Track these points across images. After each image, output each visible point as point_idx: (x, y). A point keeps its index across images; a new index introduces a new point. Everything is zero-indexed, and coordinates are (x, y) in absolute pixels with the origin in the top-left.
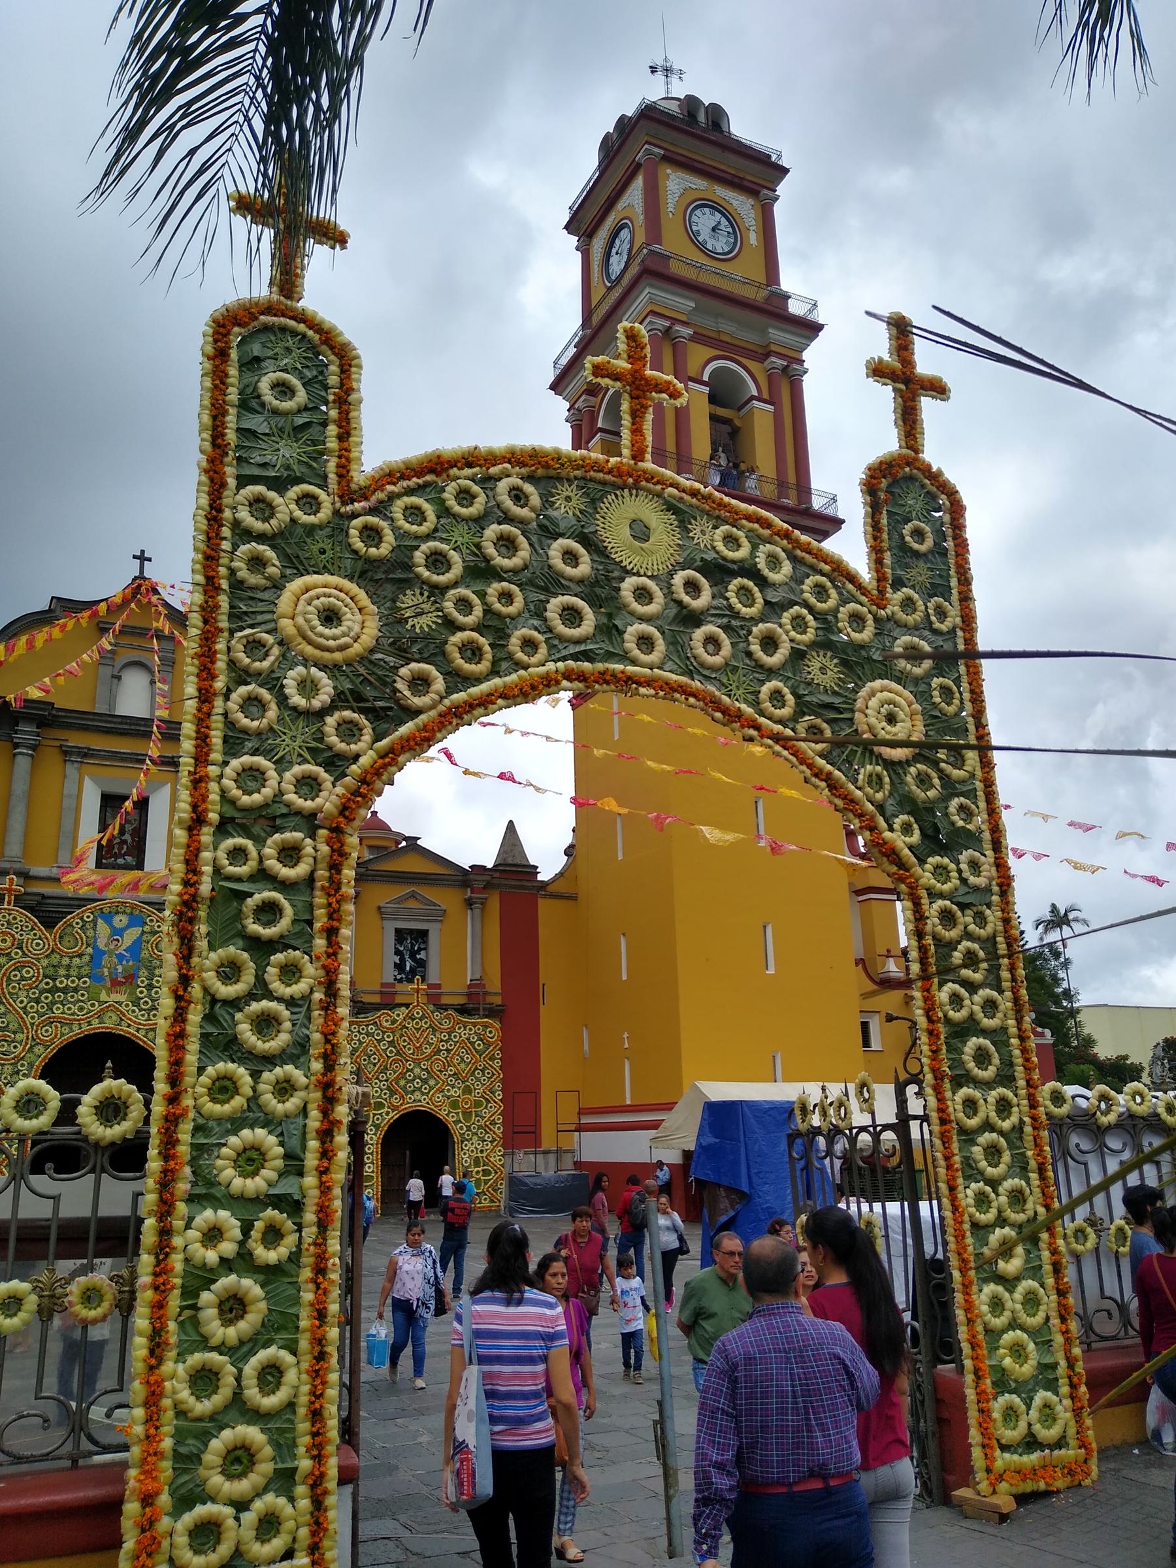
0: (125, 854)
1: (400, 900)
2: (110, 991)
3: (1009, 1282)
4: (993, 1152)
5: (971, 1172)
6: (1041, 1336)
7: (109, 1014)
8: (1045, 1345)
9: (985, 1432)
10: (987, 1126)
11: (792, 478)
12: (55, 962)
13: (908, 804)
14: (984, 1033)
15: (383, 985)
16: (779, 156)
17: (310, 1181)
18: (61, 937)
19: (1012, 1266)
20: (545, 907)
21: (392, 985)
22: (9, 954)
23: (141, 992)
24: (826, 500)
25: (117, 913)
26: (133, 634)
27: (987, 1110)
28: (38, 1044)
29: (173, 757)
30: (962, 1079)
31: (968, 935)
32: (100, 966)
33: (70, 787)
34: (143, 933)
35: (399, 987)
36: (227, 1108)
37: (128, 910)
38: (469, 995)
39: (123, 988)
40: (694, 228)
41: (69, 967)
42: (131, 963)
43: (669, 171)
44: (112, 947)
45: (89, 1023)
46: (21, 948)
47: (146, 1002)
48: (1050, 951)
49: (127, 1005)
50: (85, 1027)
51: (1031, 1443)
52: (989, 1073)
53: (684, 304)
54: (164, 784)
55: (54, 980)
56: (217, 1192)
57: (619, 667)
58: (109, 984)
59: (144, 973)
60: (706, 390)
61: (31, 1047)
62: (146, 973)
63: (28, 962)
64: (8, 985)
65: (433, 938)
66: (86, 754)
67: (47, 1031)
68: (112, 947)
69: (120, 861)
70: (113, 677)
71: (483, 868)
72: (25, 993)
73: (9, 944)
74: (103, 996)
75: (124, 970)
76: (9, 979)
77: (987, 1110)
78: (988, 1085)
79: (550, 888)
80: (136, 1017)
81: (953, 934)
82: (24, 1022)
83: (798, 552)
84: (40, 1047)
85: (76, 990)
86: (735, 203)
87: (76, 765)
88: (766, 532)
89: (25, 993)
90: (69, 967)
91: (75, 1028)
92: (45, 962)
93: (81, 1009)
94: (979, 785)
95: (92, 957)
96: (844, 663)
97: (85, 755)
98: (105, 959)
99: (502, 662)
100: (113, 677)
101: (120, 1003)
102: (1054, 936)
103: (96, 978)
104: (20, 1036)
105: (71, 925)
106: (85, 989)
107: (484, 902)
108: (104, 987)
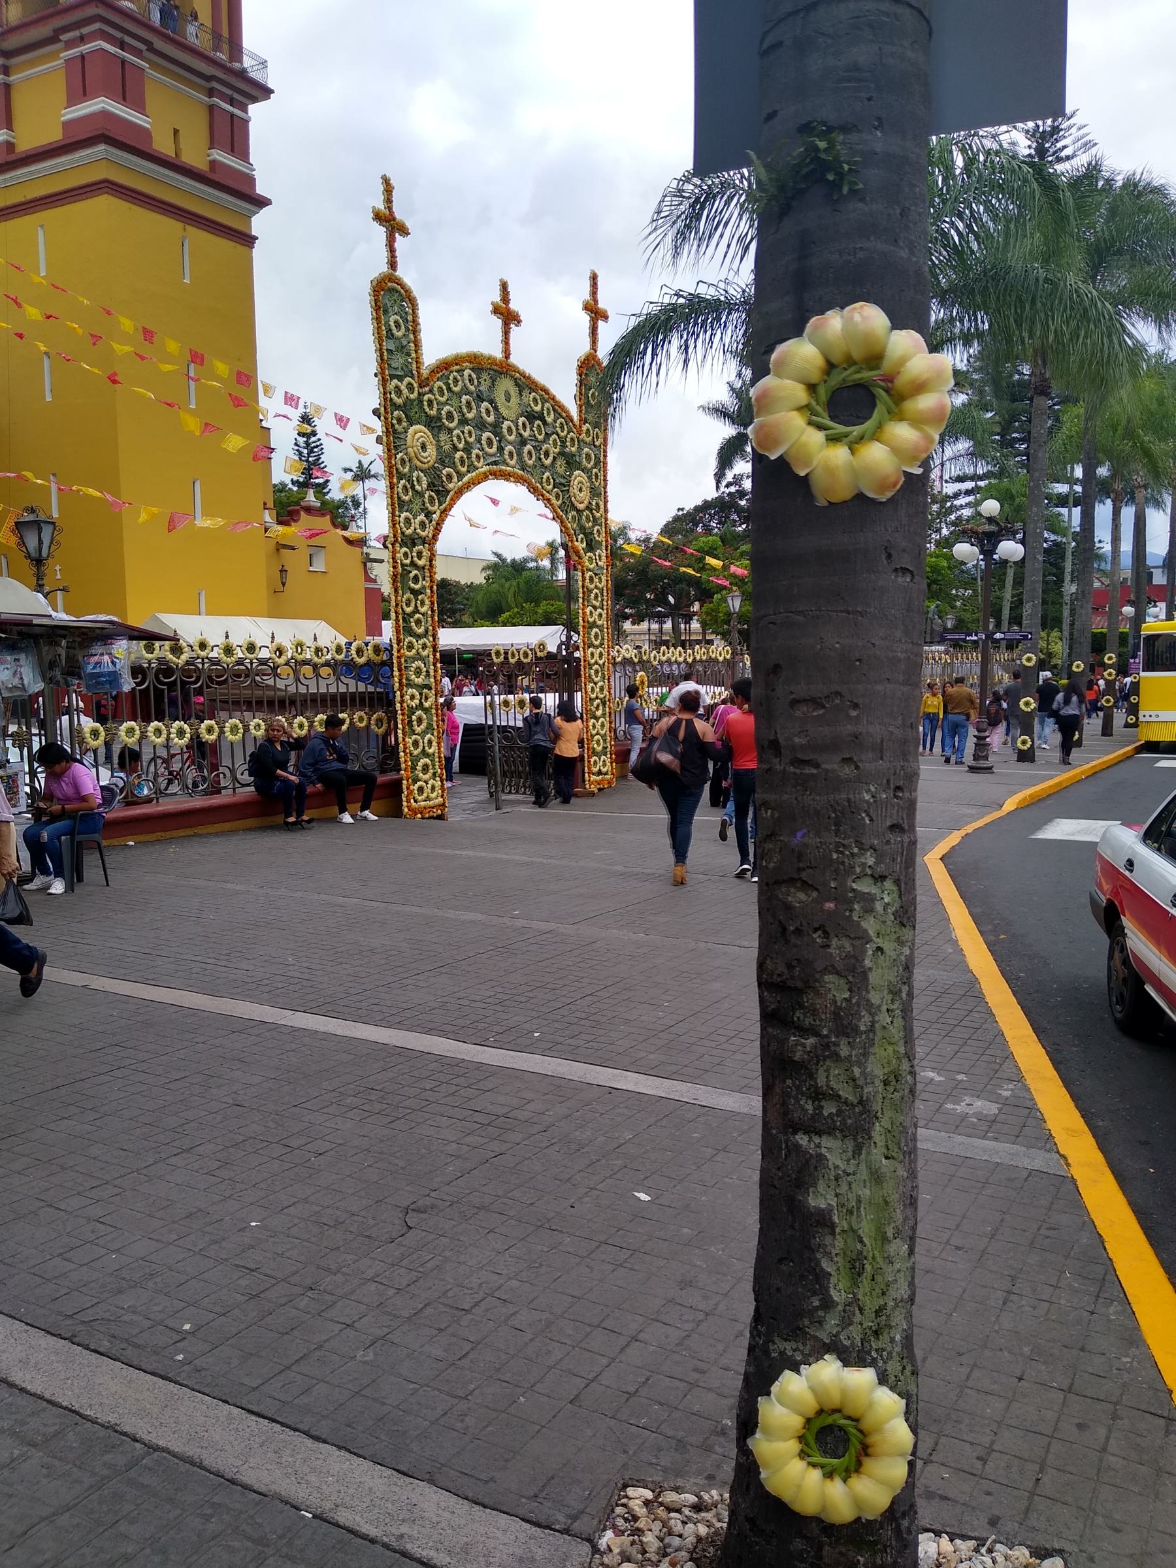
3: (597, 719)
4: (597, 672)
5: (591, 681)
6: (604, 737)
8: (605, 741)
9: (589, 769)
10: (596, 663)
11: (225, 33)
13: (583, 529)
14: (597, 627)
17: (432, 680)
19: (599, 713)
24: (256, 63)
27: (596, 656)
30: (591, 645)
31: (596, 587)
36: (411, 653)
48: (353, 501)
51: (600, 773)
52: (597, 643)
56: (412, 683)
57: (503, 468)
77: (596, 656)
78: (596, 647)
81: (592, 586)
83: (556, 407)
88: (547, 396)
94: (603, 520)
96: (567, 463)
99: (472, 468)
102: (358, 490)
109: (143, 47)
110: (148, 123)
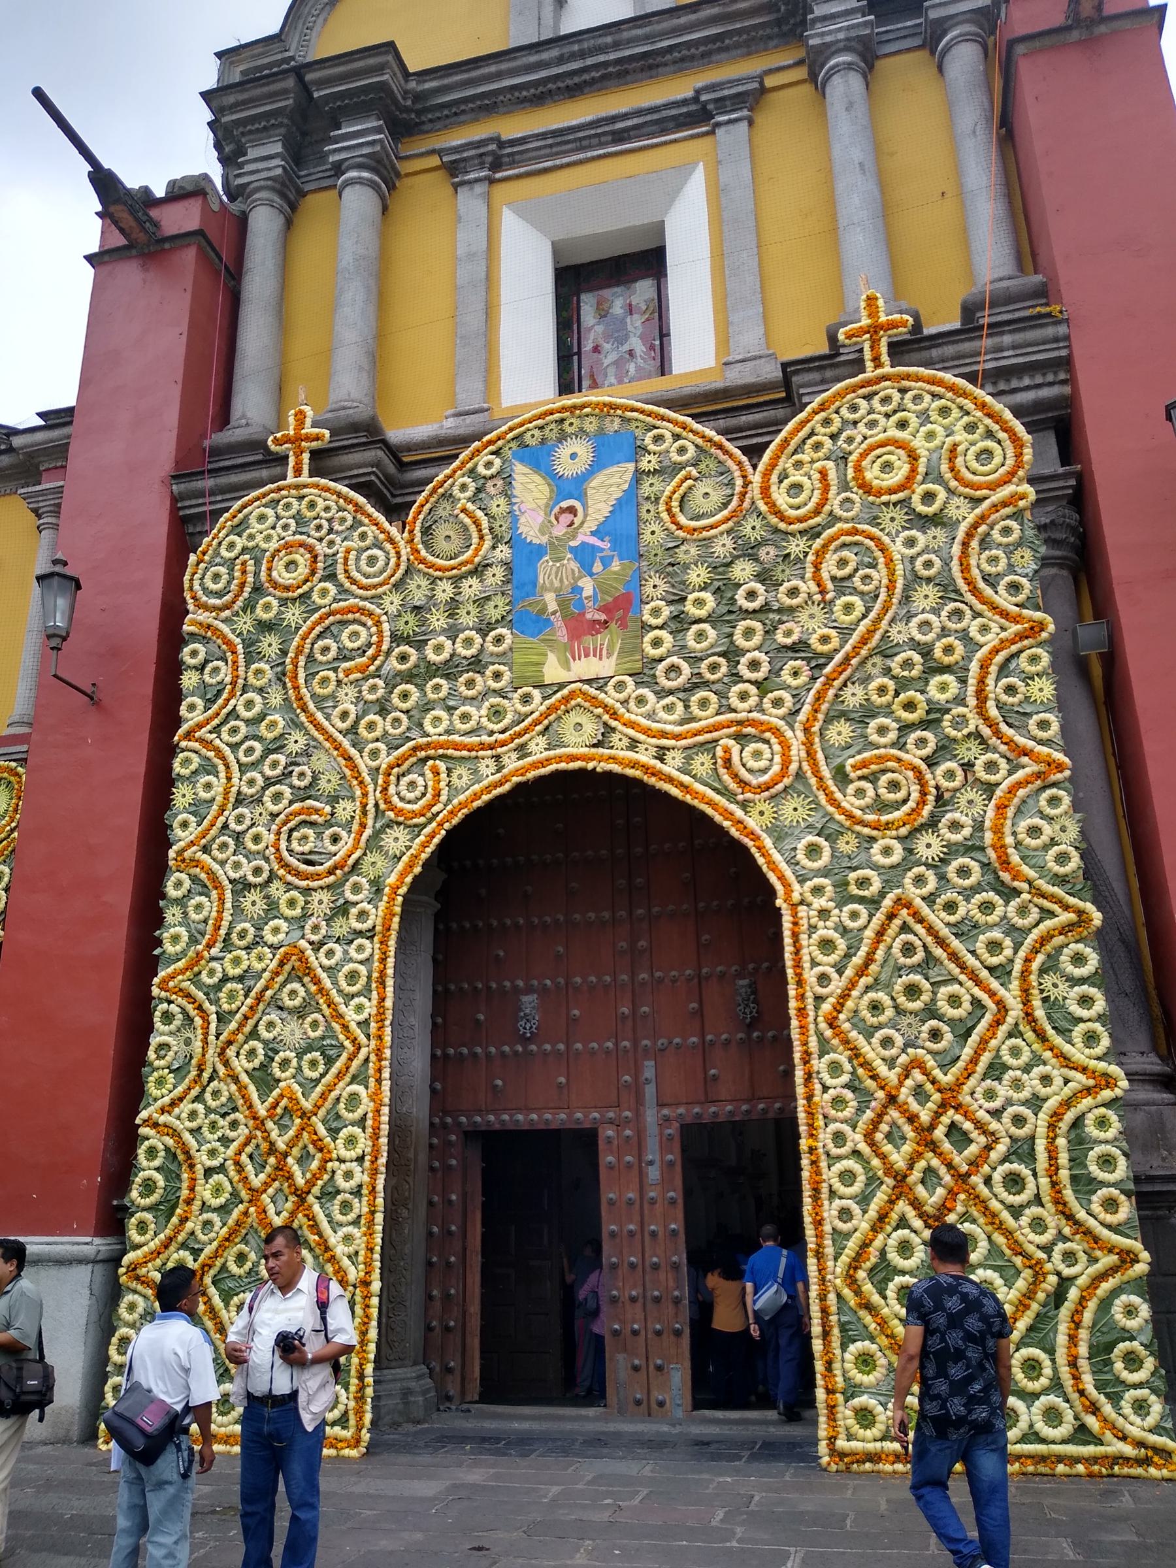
2: (571, 653)
7: (574, 718)
12: (418, 598)
18: (427, 531)
22: (306, 596)
23: (657, 643)
25: (563, 437)
28: (389, 825)
32: (532, 586)
33: (471, 237)
34: (639, 475)
37: (591, 425)
39: (603, 639)
41: (452, 607)
42: (616, 566)
44: (559, 530)
45: (523, 752)
46: (331, 577)
47: (674, 668)
49: (621, 686)
50: (512, 763)
54: (684, 171)
55: (420, 645)
58: (562, 635)
59: (656, 587)
61: (377, 834)
62: (663, 587)
63: (350, 610)
64: (310, 676)
67: (412, 784)
68: (559, 530)
72: (351, 691)
73: (303, 571)
74: (553, 671)
75: (600, 587)
76: (310, 658)
80: (650, 716)
82: (354, 767)
84: (400, 833)
85: (476, 664)
87: (479, 189)
89: (351, 691)
90: (452, 607)
91: (487, 767)
92: (393, 603)
93: (497, 713)
95: (507, 565)
98: (546, 570)
101: (599, 683)
103: (536, 622)
104: (345, 809)
105: (448, 496)
106: (502, 658)
108: (550, 643)
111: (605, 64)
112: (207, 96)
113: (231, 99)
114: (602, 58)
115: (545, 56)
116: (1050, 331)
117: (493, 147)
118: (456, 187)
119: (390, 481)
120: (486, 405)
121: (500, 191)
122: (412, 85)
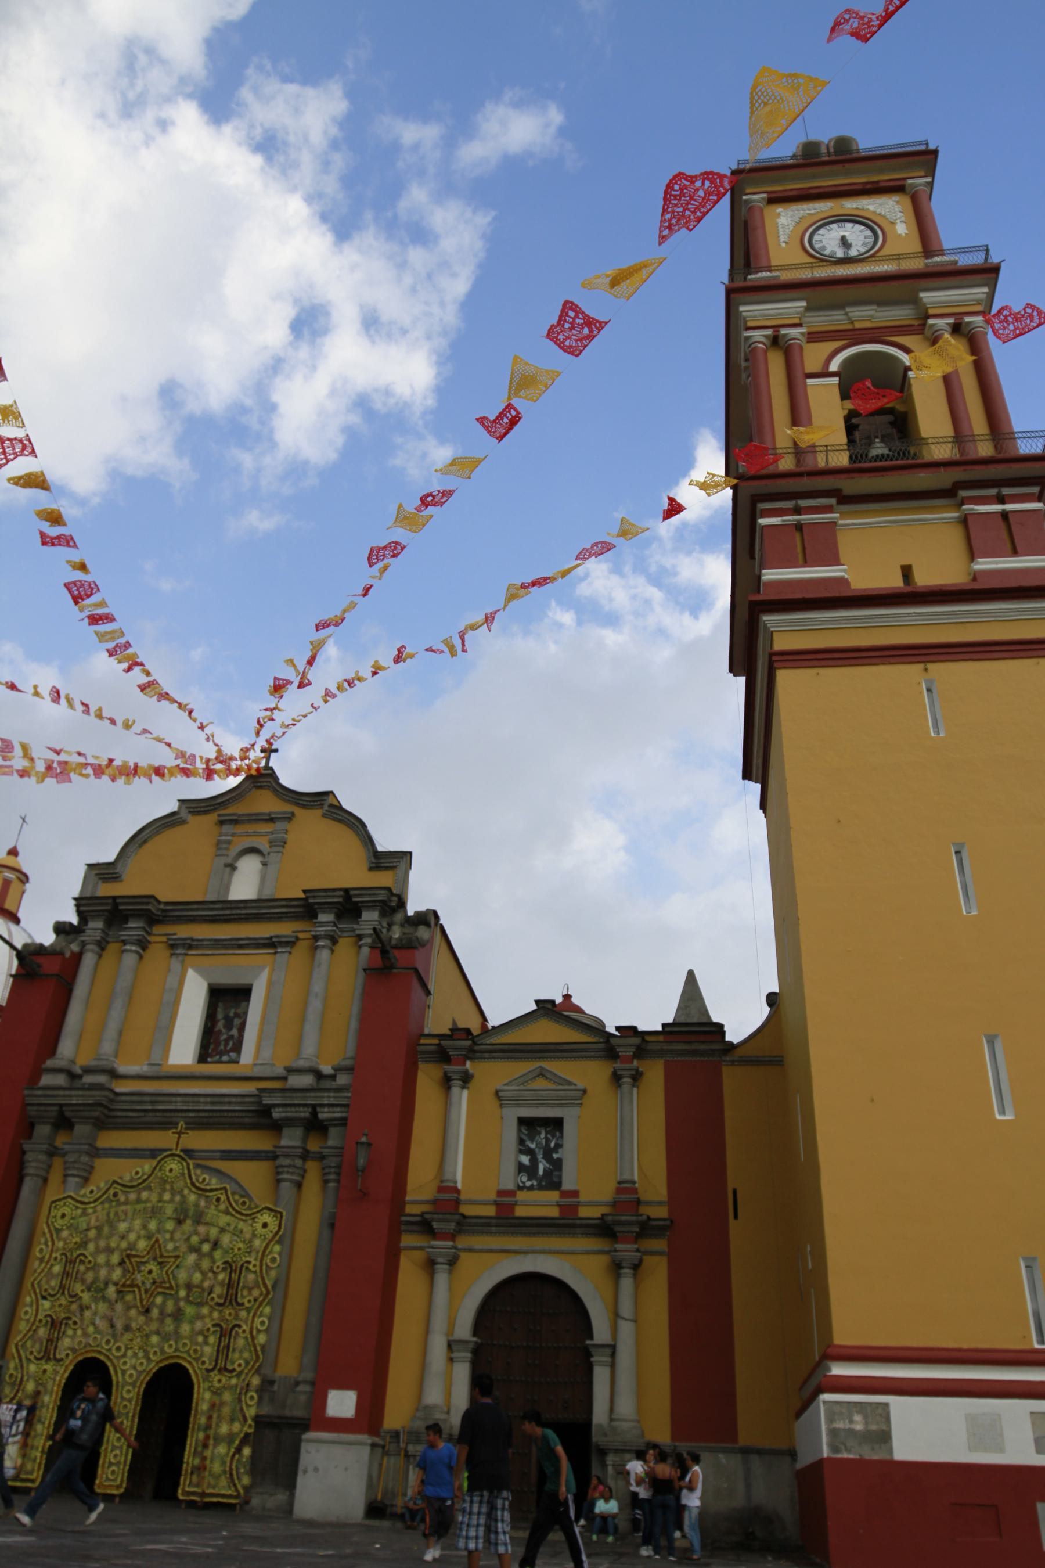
0: (229, 1051)
1: (524, 1079)
15: (501, 1193)
16: (927, 144)
20: (731, 1078)
21: (511, 1193)
26: (250, 821)
29: (271, 938)
33: (172, 981)
35: (521, 1196)
38: (614, 1204)
40: (817, 246)
43: (779, 210)
53: (794, 306)
54: (262, 968)
60: (835, 380)
65: (567, 1127)
66: (190, 945)
69: (225, 1058)
70: (227, 865)
71: (633, 1029)
79: (739, 1052)
86: (871, 208)
87: (181, 958)
97: (190, 947)
100: (227, 865)
107: (637, 1077)
109: (833, 501)
110: (844, 571)
111: (240, 914)
112: (75, 899)
113: (84, 902)
114: (239, 911)
115: (217, 906)
116: (346, 1094)
117: (189, 942)
118: (172, 955)
119: (111, 1101)
120: (161, 1062)
121: (188, 959)
122: (162, 907)
